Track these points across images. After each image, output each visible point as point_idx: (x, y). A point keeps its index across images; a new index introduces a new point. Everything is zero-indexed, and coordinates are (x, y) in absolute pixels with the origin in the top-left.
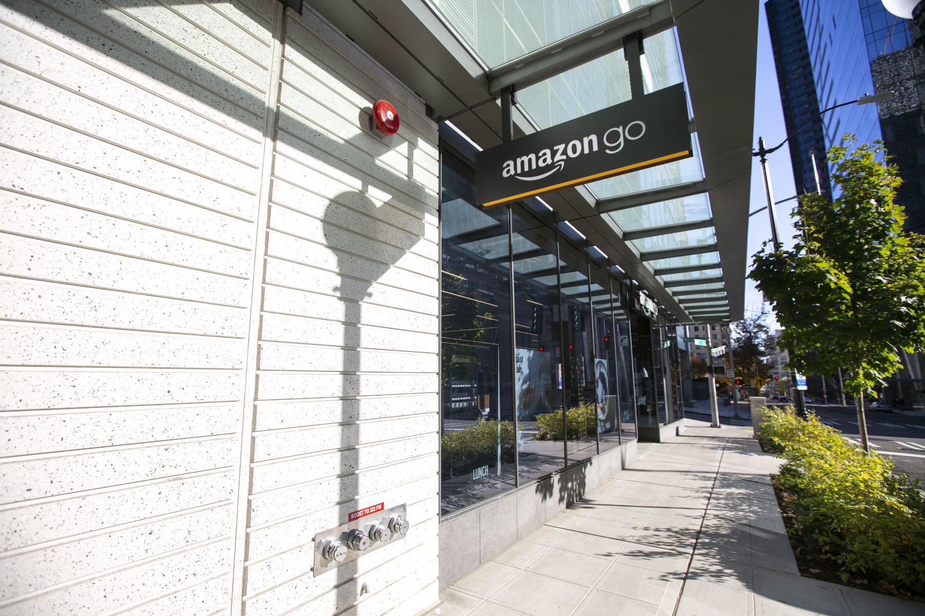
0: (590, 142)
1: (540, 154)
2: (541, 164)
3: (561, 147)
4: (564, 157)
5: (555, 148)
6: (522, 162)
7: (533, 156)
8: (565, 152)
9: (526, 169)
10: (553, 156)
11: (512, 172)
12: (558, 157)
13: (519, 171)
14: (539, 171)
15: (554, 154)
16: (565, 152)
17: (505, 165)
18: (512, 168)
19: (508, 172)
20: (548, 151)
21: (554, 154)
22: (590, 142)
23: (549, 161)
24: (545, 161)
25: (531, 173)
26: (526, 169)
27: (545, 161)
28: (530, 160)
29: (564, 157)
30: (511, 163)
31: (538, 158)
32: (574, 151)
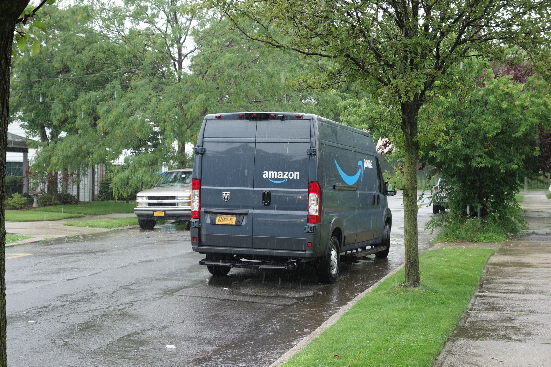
0: (297, 174)
1: (279, 173)
2: (279, 177)
3: (286, 173)
4: (287, 177)
5: (285, 172)
6: (271, 174)
7: (276, 172)
8: (288, 175)
9: (273, 177)
10: (283, 176)
11: (267, 177)
12: (285, 176)
13: (270, 177)
14: (278, 179)
15: (284, 174)
16: (288, 175)
17: (264, 172)
18: (267, 174)
19: (266, 176)
20: (281, 173)
21: (284, 174)
22: (297, 174)
23: (282, 177)
24: (280, 176)
25: (274, 179)
26: (273, 177)
27: (280, 176)
28: (274, 174)
29: (287, 177)
30: (267, 172)
31: (278, 174)
32: (291, 176)
